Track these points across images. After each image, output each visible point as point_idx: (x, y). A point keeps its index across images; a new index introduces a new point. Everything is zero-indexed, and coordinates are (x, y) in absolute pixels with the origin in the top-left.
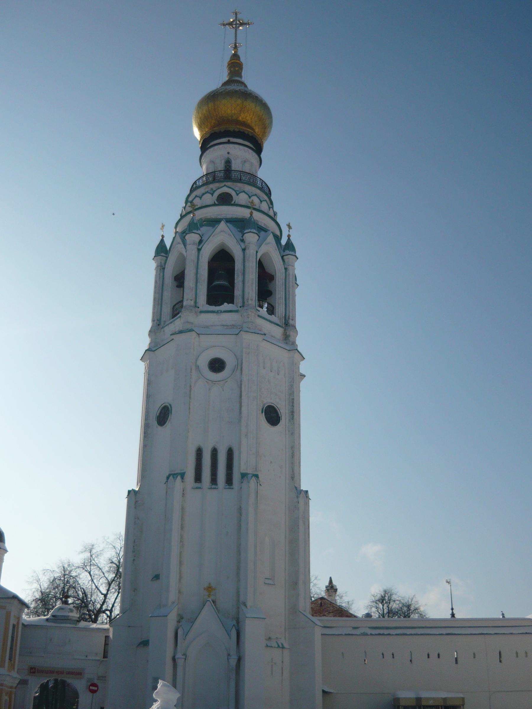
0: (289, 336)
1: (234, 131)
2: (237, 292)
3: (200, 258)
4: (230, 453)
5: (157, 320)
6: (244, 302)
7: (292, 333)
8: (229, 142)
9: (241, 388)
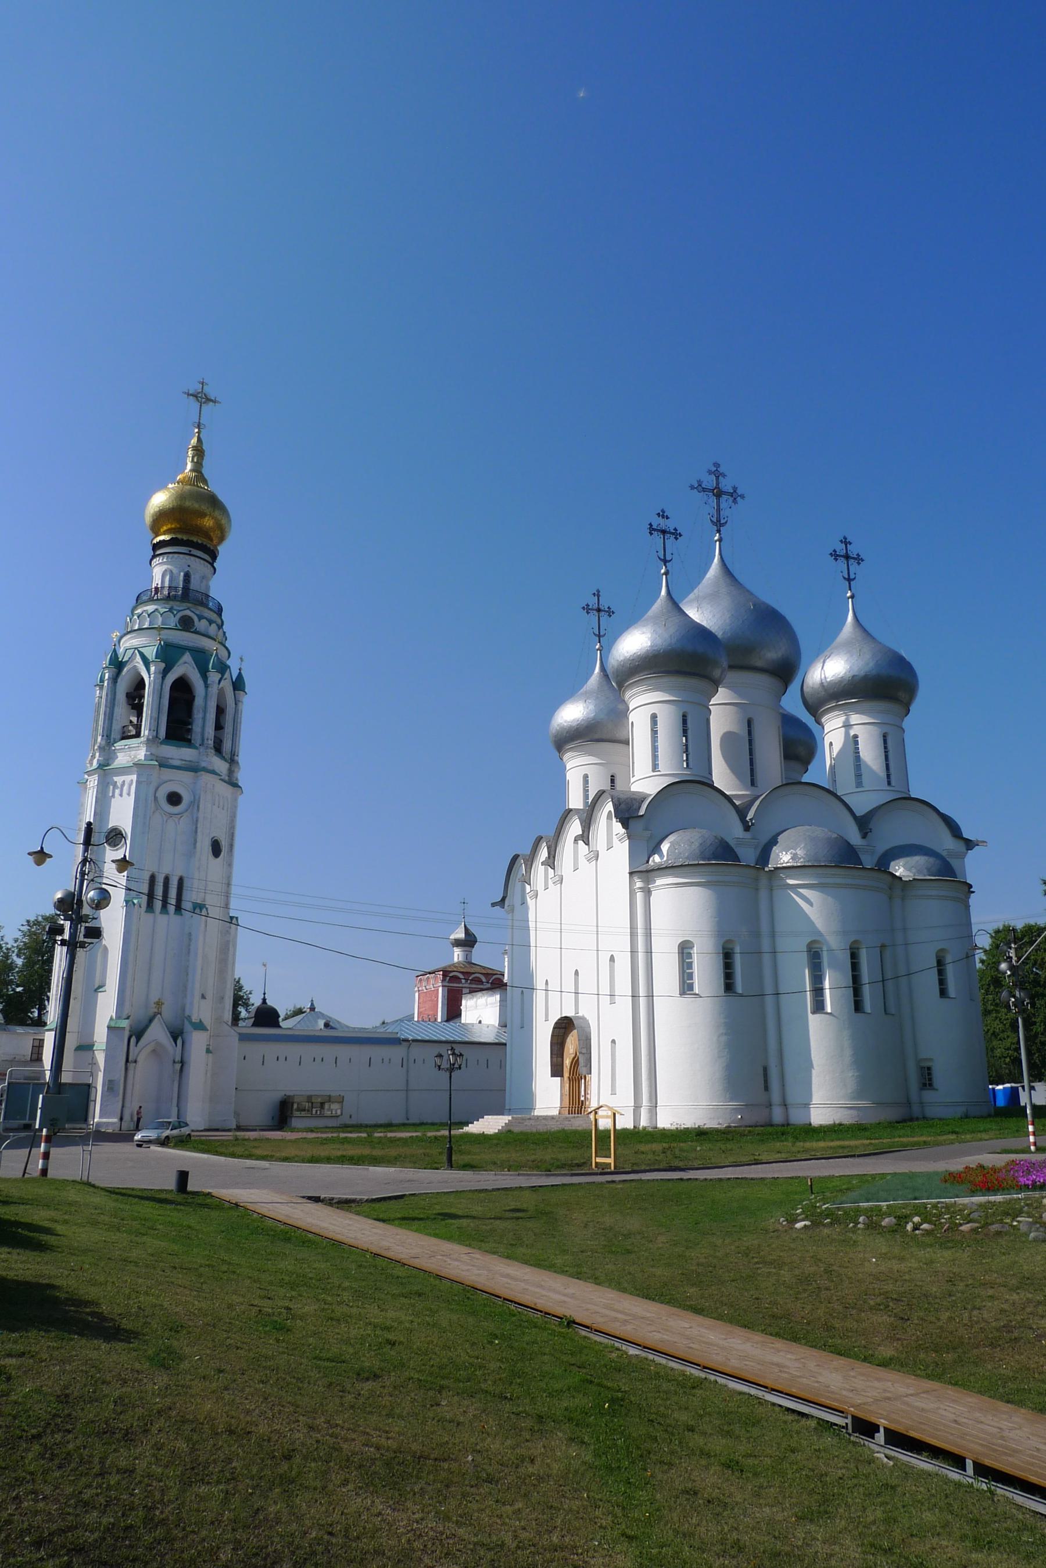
0: (234, 771)
1: (197, 542)
2: (196, 727)
3: (164, 687)
4: (181, 881)
5: (107, 736)
6: (203, 740)
7: (236, 770)
9: (196, 824)
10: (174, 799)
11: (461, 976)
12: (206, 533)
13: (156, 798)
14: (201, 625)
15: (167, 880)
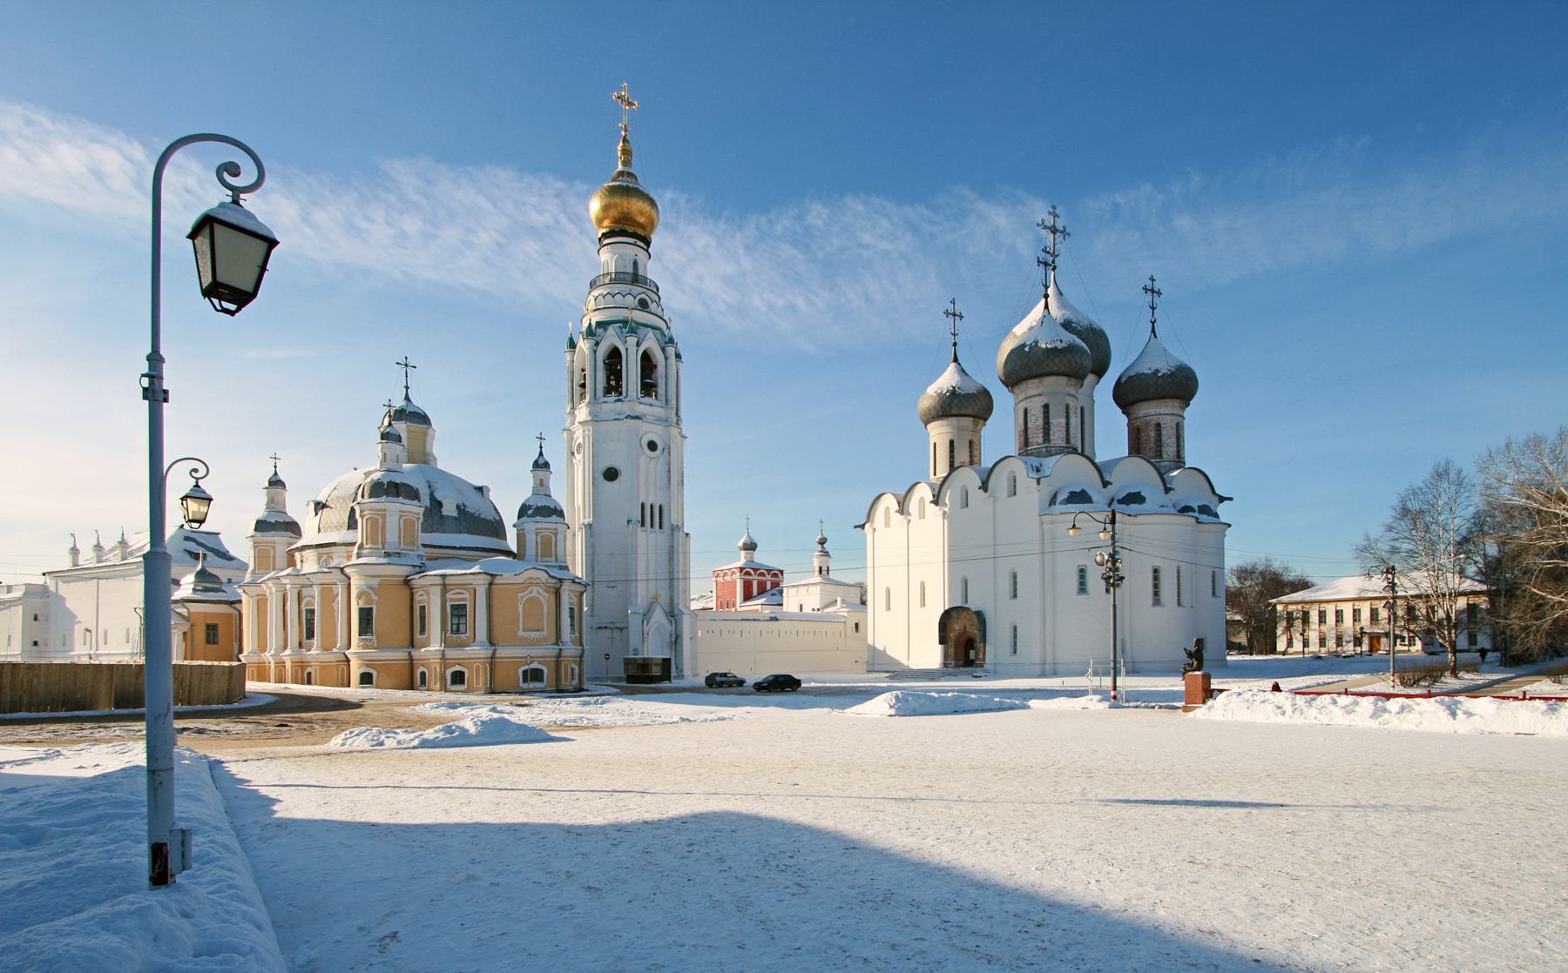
8: (635, 245)
10: (652, 446)
11: (765, 572)
12: (642, 227)
13: (641, 445)
14: (653, 307)
15: (652, 506)
